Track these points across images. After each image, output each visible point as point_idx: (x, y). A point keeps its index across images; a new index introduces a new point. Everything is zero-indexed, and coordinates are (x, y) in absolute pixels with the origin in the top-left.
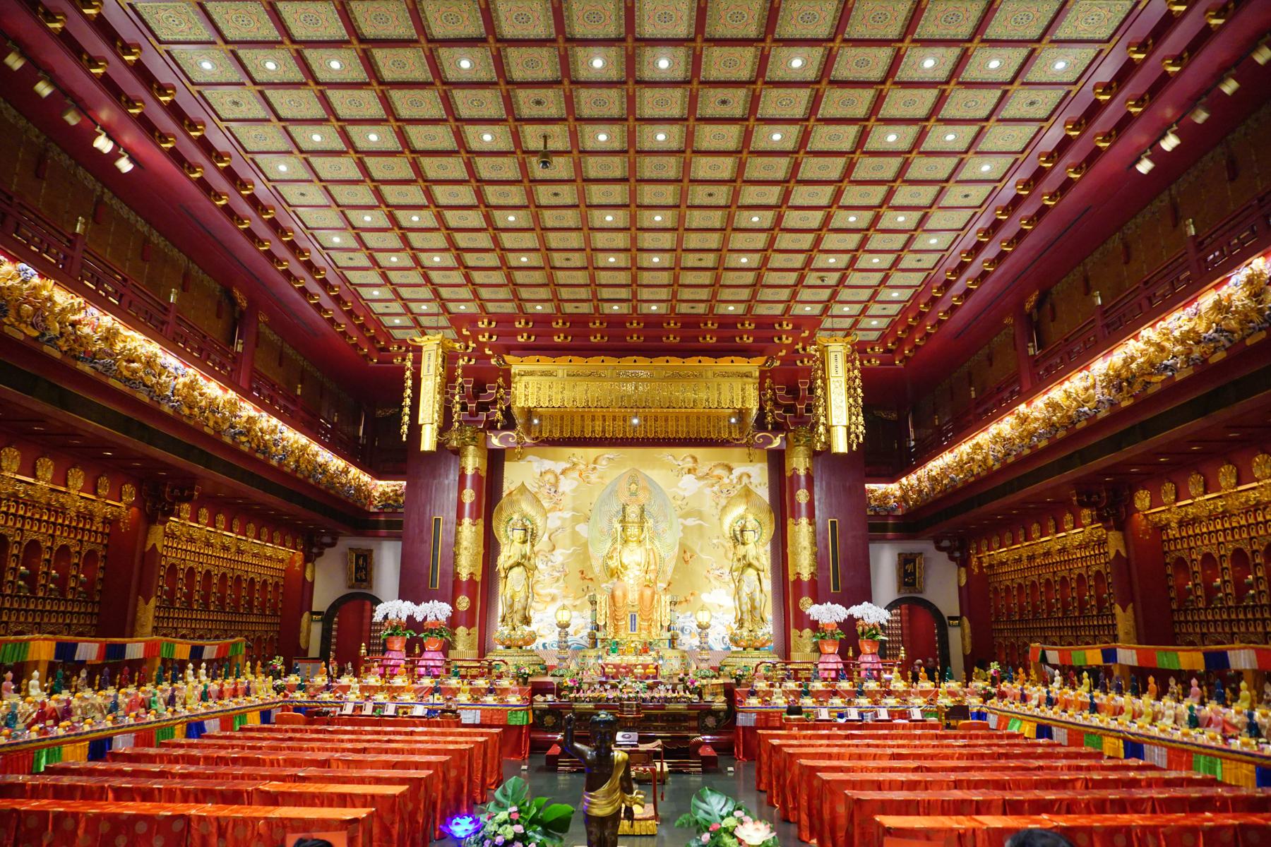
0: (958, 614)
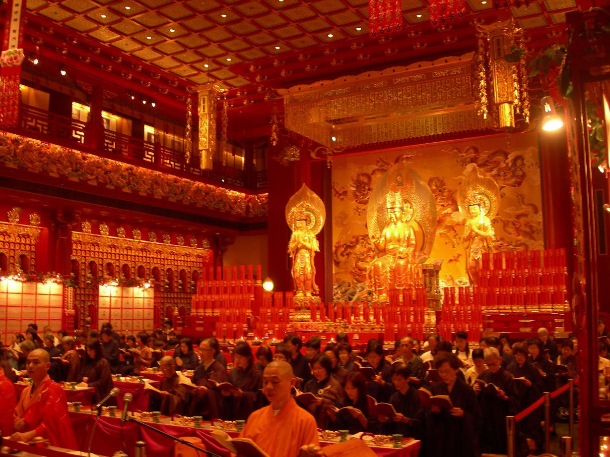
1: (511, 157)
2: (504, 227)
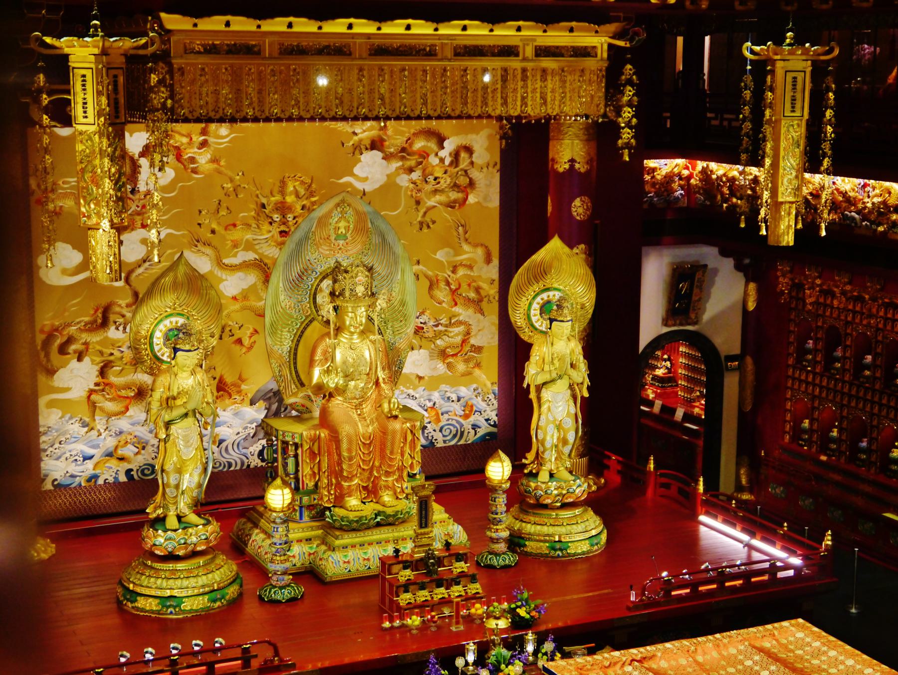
0: (736, 350)
1: (450, 145)
2: (431, 288)
